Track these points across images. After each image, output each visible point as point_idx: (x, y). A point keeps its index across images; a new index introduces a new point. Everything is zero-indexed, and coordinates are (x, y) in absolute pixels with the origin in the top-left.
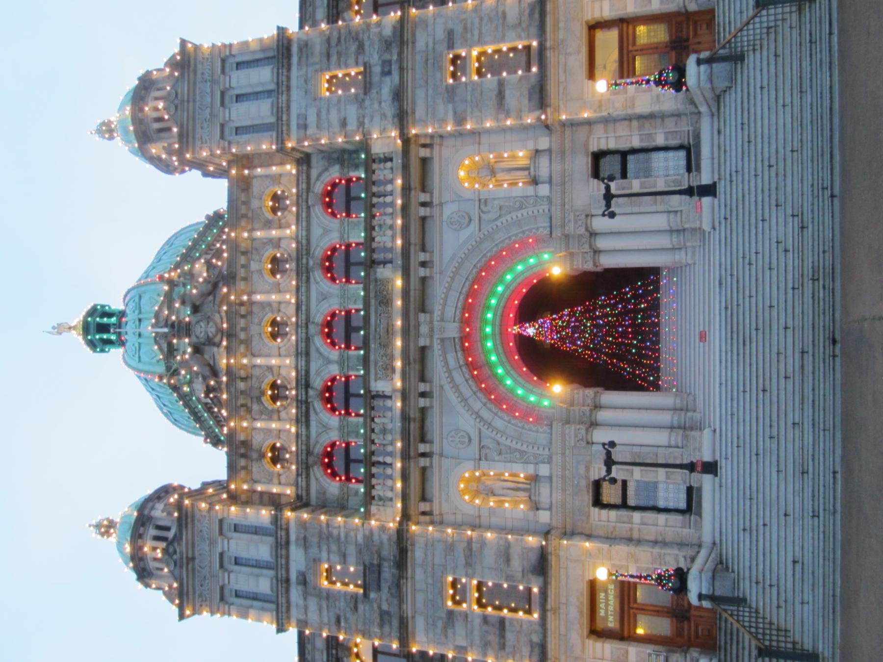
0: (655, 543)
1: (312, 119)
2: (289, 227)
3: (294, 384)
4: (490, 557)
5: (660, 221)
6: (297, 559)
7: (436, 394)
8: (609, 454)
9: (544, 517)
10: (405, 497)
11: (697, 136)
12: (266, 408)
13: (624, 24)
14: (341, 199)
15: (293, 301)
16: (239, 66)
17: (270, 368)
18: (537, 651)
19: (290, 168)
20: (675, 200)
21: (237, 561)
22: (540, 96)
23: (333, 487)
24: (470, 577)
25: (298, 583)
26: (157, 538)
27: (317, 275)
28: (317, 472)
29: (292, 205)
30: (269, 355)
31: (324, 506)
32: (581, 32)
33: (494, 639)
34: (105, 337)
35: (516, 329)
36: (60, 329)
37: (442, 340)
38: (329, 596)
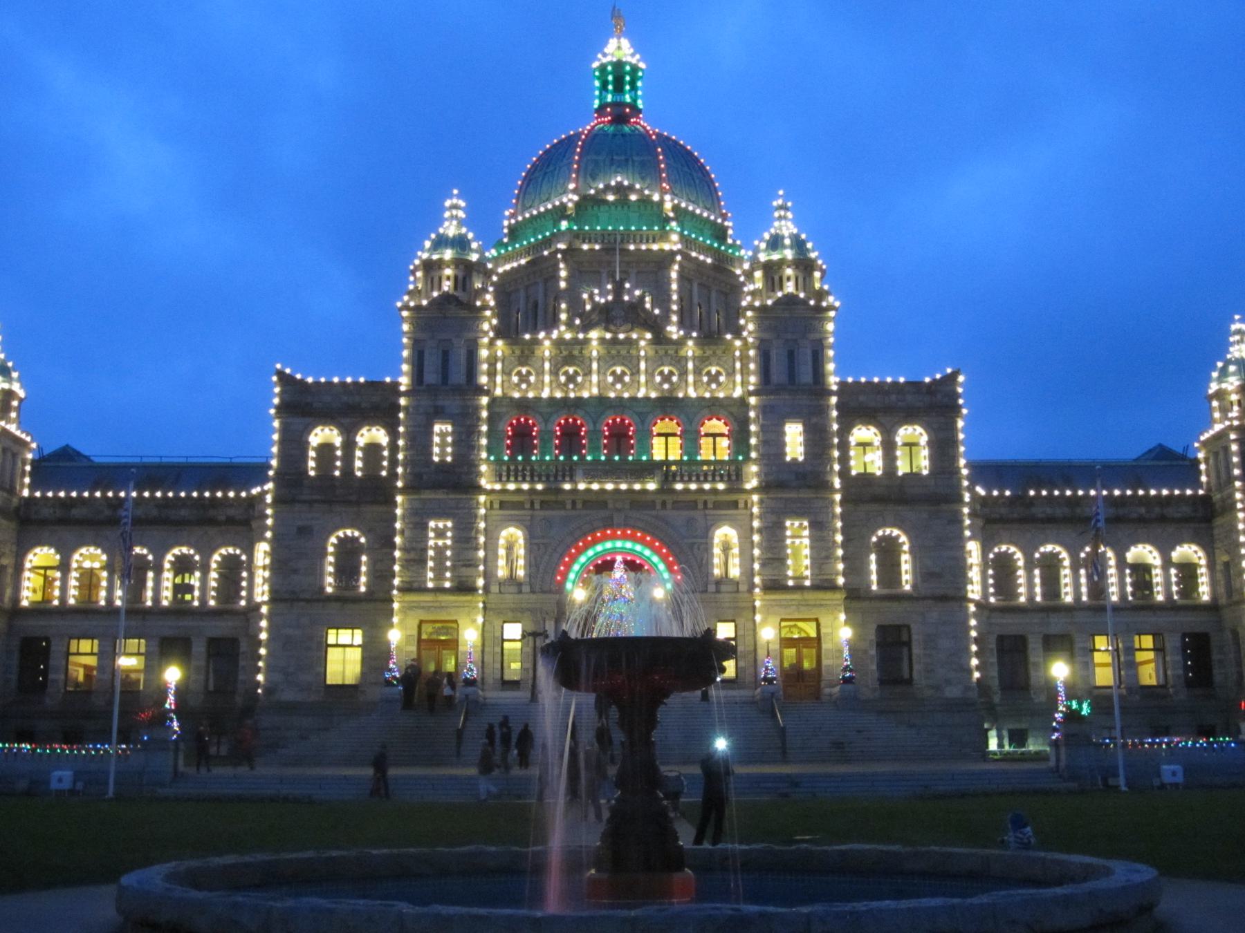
0: (483, 662)
2: (695, 390)
3: (578, 394)
7: (574, 512)
8: (540, 634)
10: (504, 491)
12: (559, 370)
15: (640, 395)
17: (588, 373)
18: (407, 586)
19: (738, 393)
24: (453, 538)
25: (436, 407)
26: (456, 278)
29: (712, 391)
30: (599, 372)
31: (491, 420)
33: (412, 555)
34: (610, 87)
35: (619, 558)
37: (611, 518)
38: (430, 433)
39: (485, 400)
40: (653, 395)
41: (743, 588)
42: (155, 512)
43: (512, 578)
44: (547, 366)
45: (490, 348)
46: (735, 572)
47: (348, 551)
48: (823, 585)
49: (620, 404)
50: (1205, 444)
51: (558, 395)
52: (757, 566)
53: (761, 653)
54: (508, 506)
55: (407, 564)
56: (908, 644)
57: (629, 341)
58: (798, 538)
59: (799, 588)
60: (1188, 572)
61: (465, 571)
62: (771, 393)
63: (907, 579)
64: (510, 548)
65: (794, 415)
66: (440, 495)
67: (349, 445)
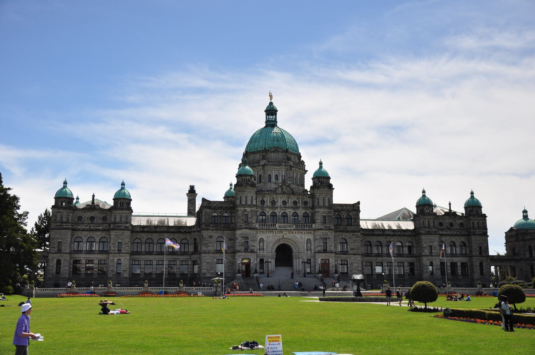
1: (319, 214)
4: (253, 244)
5: (301, 269)
6: (248, 209)
9: (258, 251)
11: (312, 274)
13: (329, 264)
14: (306, 216)
16: (329, 199)
20: (304, 271)
21: (246, 197)
22: (319, 252)
23: (258, 214)
27: (293, 211)
28: (261, 211)
32: (328, 258)
36: (271, 96)
42: (166, 230)
53: (317, 267)
56: (347, 264)
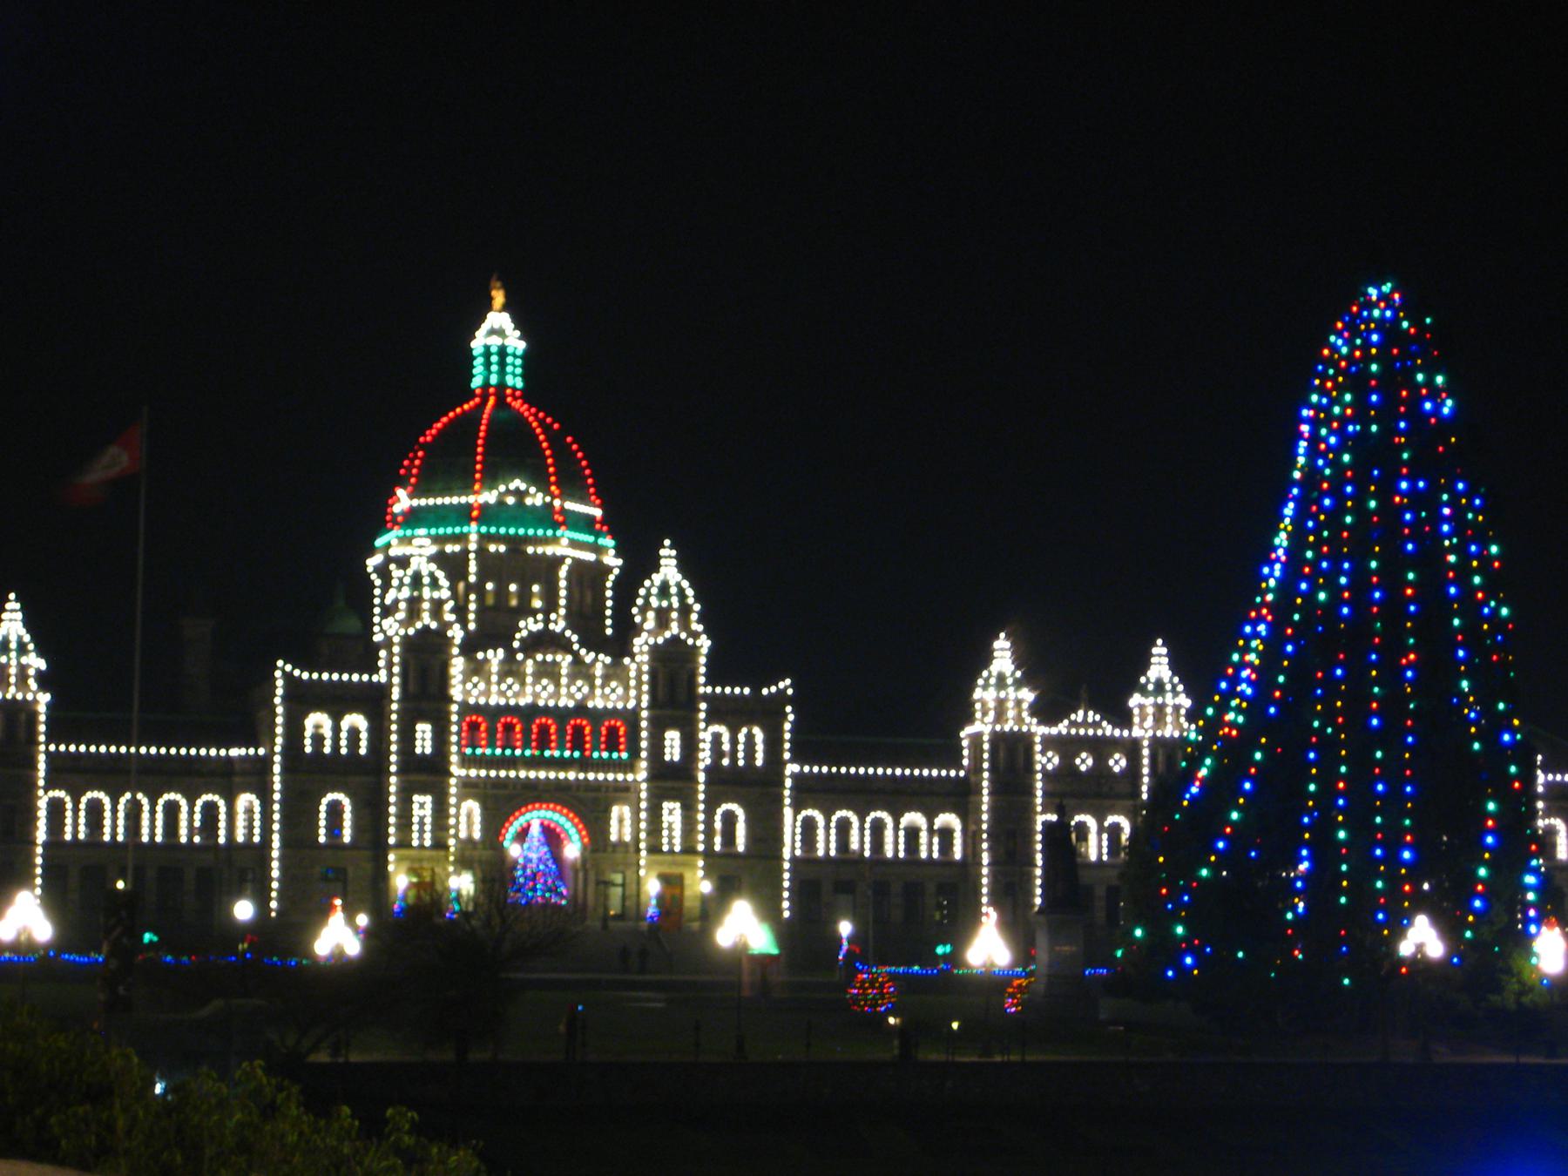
17: (523, 684)
19: (631, 704)
39: (454, 708)
40: (571, 704)
41: (632, 849)
43: (470, 839)
44: (494, 678)
45: (458, 665)
46: (627, 838)
47: (335, 809)
48: (689, 849)
49: (546, 711)
50: (970, 736)
51: (502, 702)
52: (643, 835)
54: (470, 788)
55: (399, 827)
57: (554, 663)
58: (672, 813)
59: (671, 852)
60: (946, 834)
61: (440, 834)
62: (661, 708)
63: (741, 845)
64: (469, 816)
65: (673, 726)
66: (423, 778)
67: (336, 730)
